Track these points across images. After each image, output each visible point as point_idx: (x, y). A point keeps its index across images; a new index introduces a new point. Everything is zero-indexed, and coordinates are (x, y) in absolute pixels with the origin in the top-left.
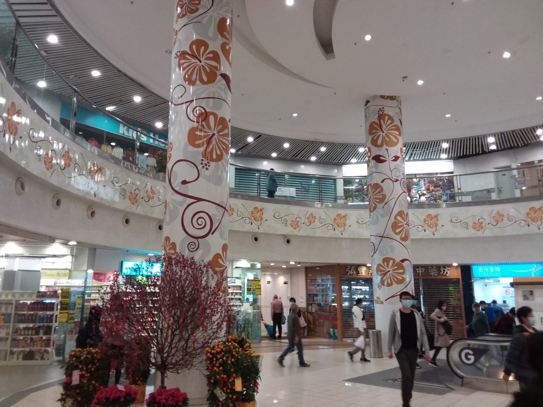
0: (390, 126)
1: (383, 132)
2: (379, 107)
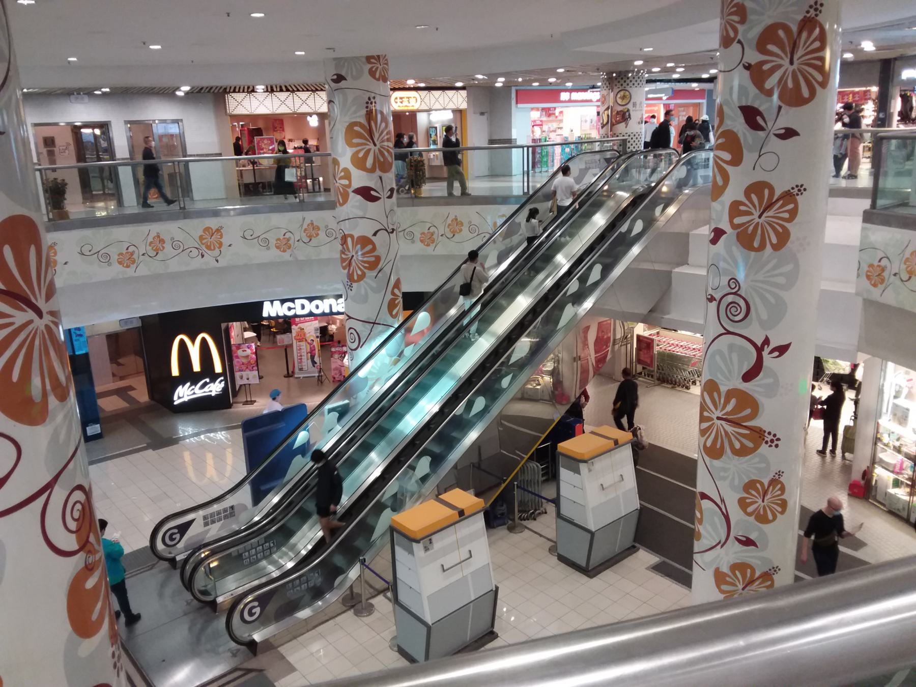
2: (368, 95)
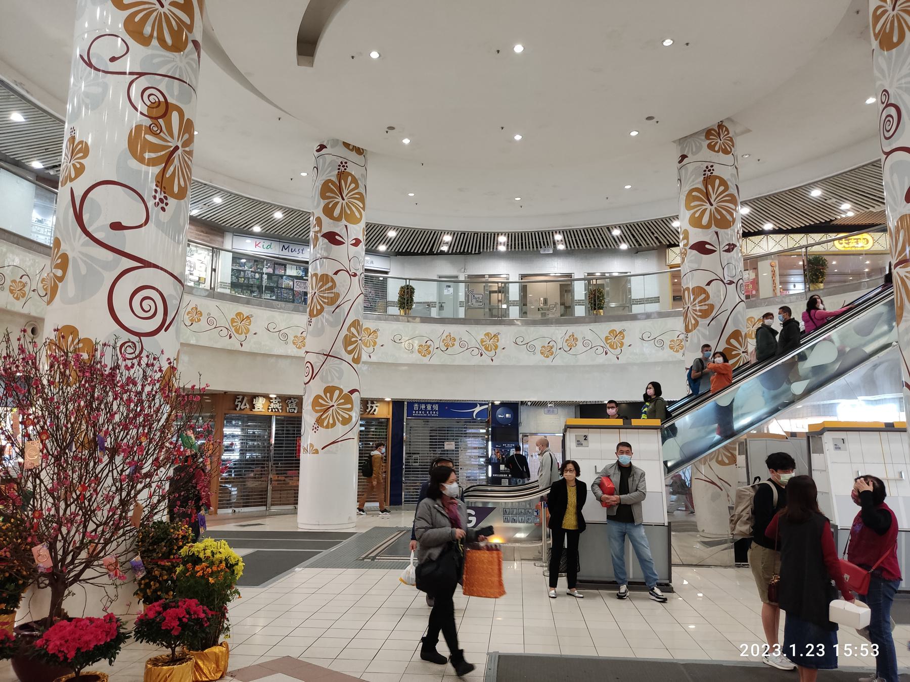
0: (353, 192)
1: (343, 199)
